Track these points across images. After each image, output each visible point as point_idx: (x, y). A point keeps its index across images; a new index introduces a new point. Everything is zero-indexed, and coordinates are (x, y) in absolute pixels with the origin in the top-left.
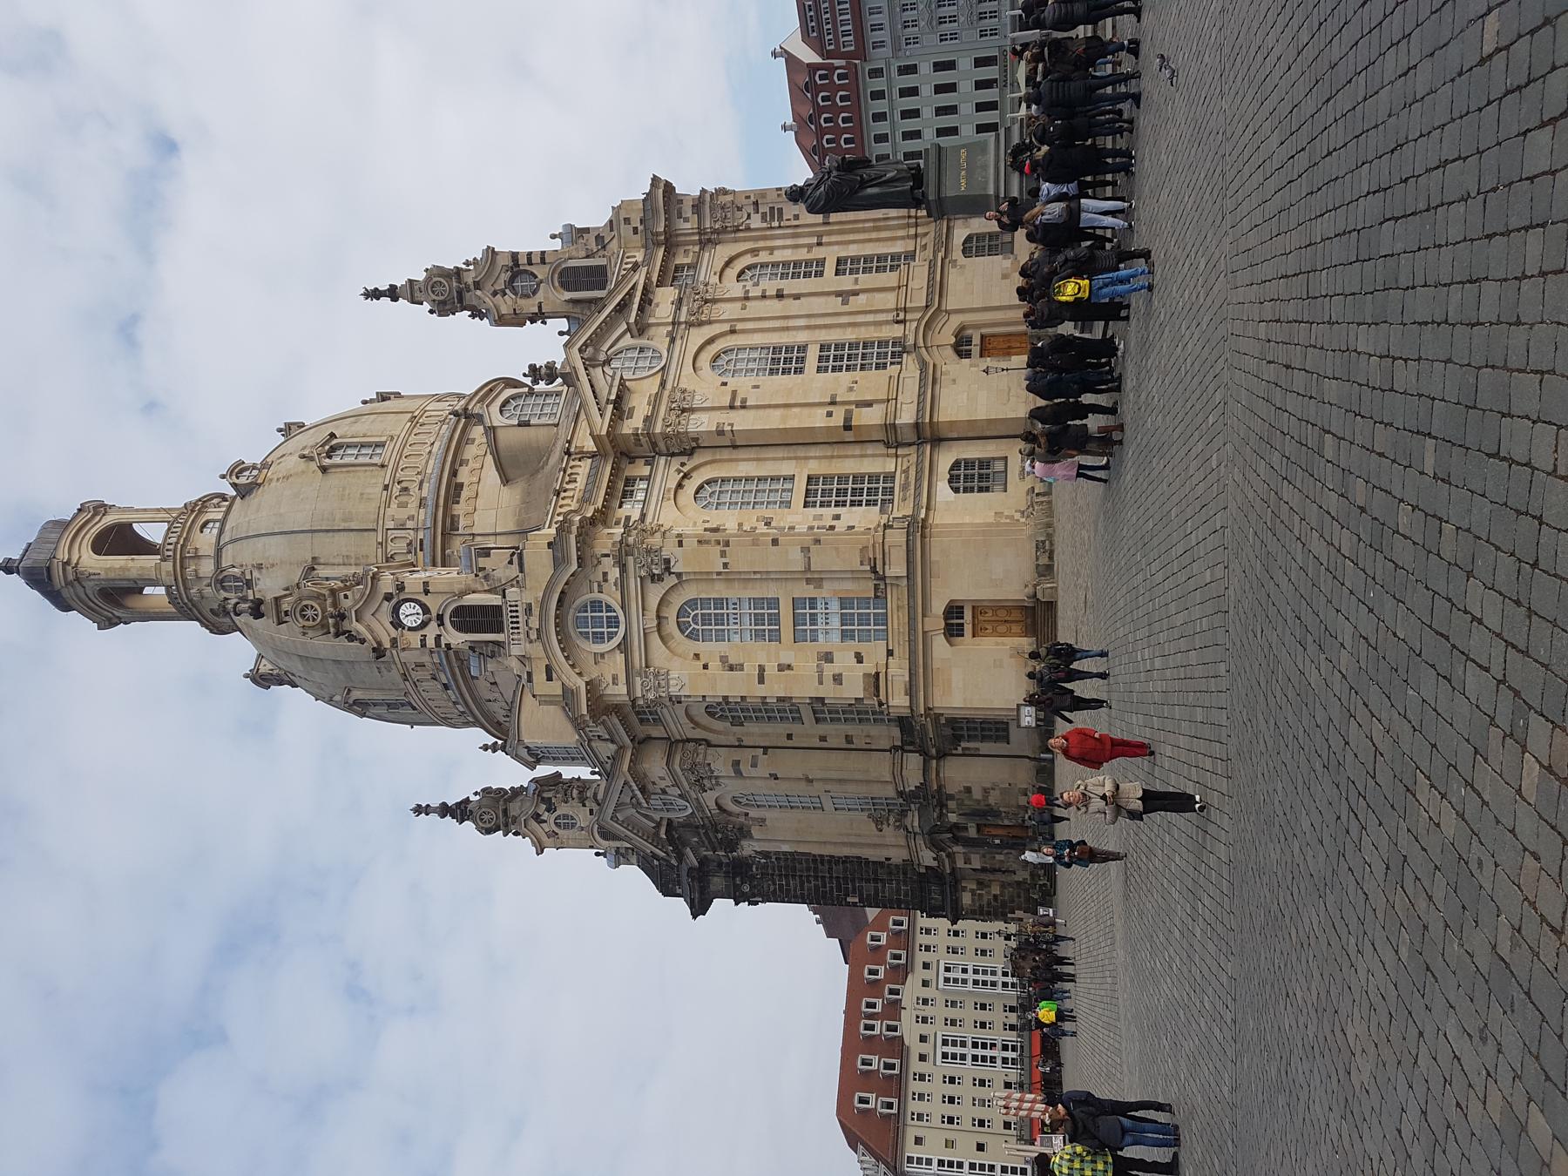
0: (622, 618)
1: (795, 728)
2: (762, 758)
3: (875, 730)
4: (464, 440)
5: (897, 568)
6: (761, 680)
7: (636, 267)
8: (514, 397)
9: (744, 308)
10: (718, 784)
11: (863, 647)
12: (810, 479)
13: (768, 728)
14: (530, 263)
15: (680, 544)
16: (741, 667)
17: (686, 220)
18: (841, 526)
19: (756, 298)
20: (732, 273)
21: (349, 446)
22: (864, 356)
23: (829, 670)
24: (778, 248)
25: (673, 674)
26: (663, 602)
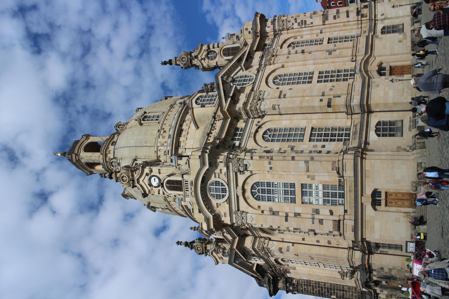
0: (227, 189)
2: (292, 248)
4: (186, 113)
5: (349, 173)
6: (286, 220)
8: (201, 96)
9: (288, 57)
11: (333, 208)
14: (214, 48)
15: (252, 158)
17: (269, 27)
18: (324, 150)
19: (293, 54)
20: (285, 45)
22: (338, 76)
24: (305, 35)
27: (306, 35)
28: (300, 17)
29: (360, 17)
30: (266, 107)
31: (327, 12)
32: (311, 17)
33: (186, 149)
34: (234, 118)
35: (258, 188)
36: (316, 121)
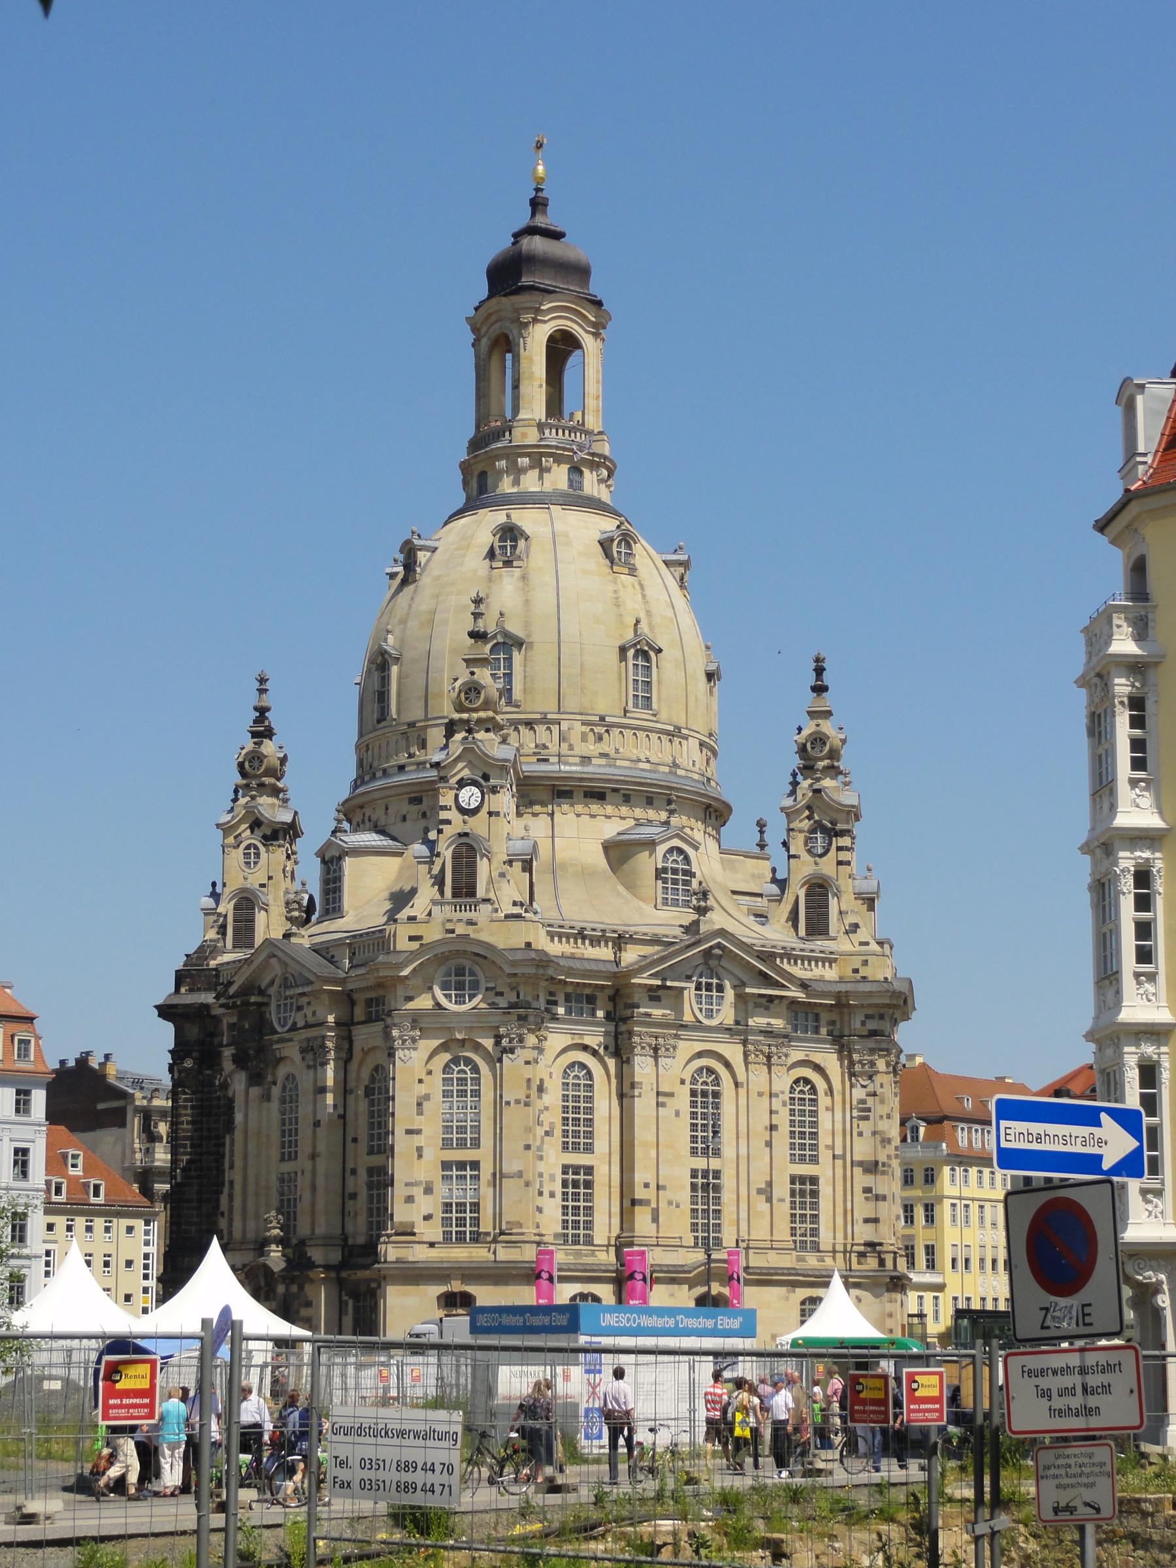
1: (363, 1146)
3: (362, 1220)
5: (504, 1254)
6: (409, 1132)
7: (804, 985)
8: (687, 860)
9: (760, 1094)
10: (309, 1067)
12: (589, 1170)
13: (363, 1121)
14: (839, 849)
15: (527, 1063)
16: (420, 1113)
17: (863, 1023)
21: (649, 668)
23: (418, 1192)
25: (413, 1054)
26: (477, 1047)
27: (830, 1122)
28: (879, 1107)
29: (862, 1248)
30: (637, 1067)
31: (884, 1173)
32: (874, 1133)
33: (553, 814)
34: (618, 990)
35: (467, 1069)
36: (606, 1173)
